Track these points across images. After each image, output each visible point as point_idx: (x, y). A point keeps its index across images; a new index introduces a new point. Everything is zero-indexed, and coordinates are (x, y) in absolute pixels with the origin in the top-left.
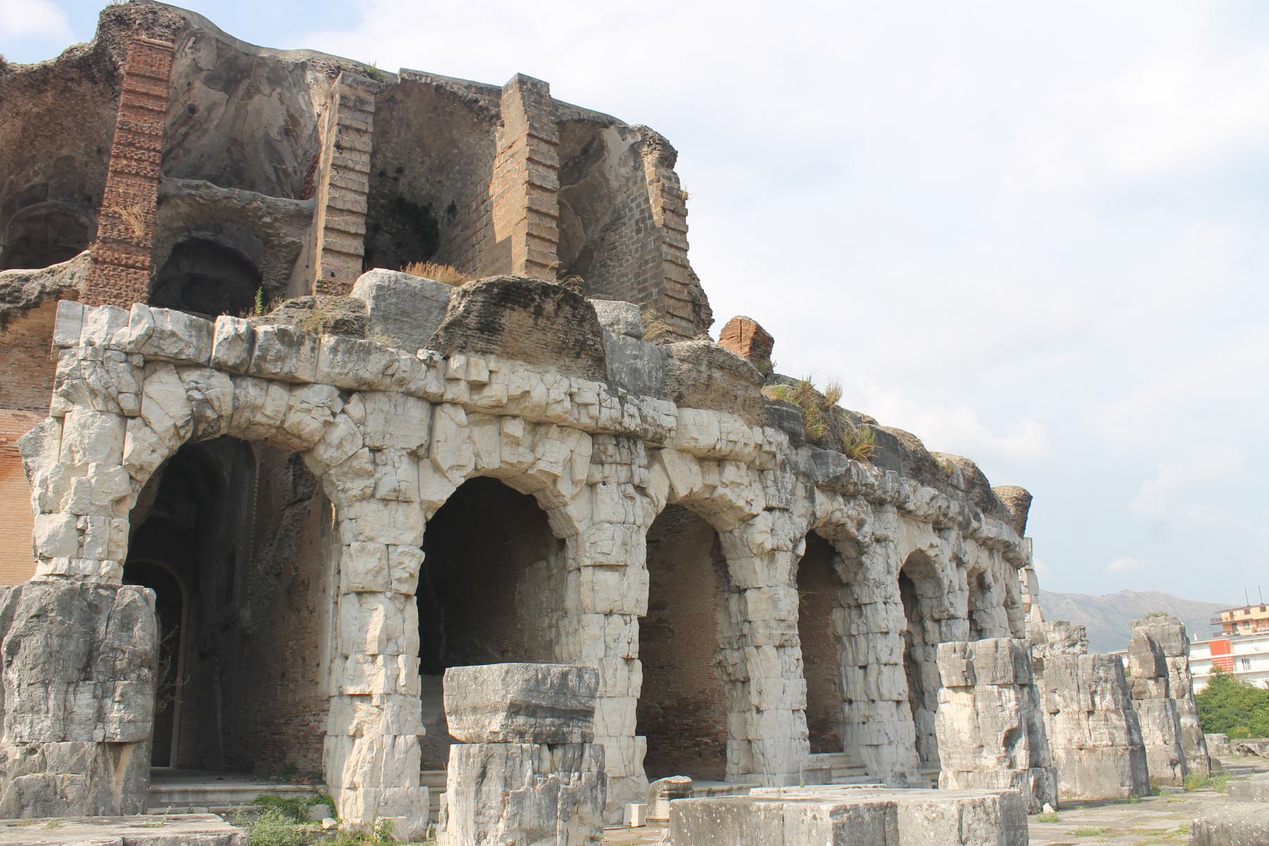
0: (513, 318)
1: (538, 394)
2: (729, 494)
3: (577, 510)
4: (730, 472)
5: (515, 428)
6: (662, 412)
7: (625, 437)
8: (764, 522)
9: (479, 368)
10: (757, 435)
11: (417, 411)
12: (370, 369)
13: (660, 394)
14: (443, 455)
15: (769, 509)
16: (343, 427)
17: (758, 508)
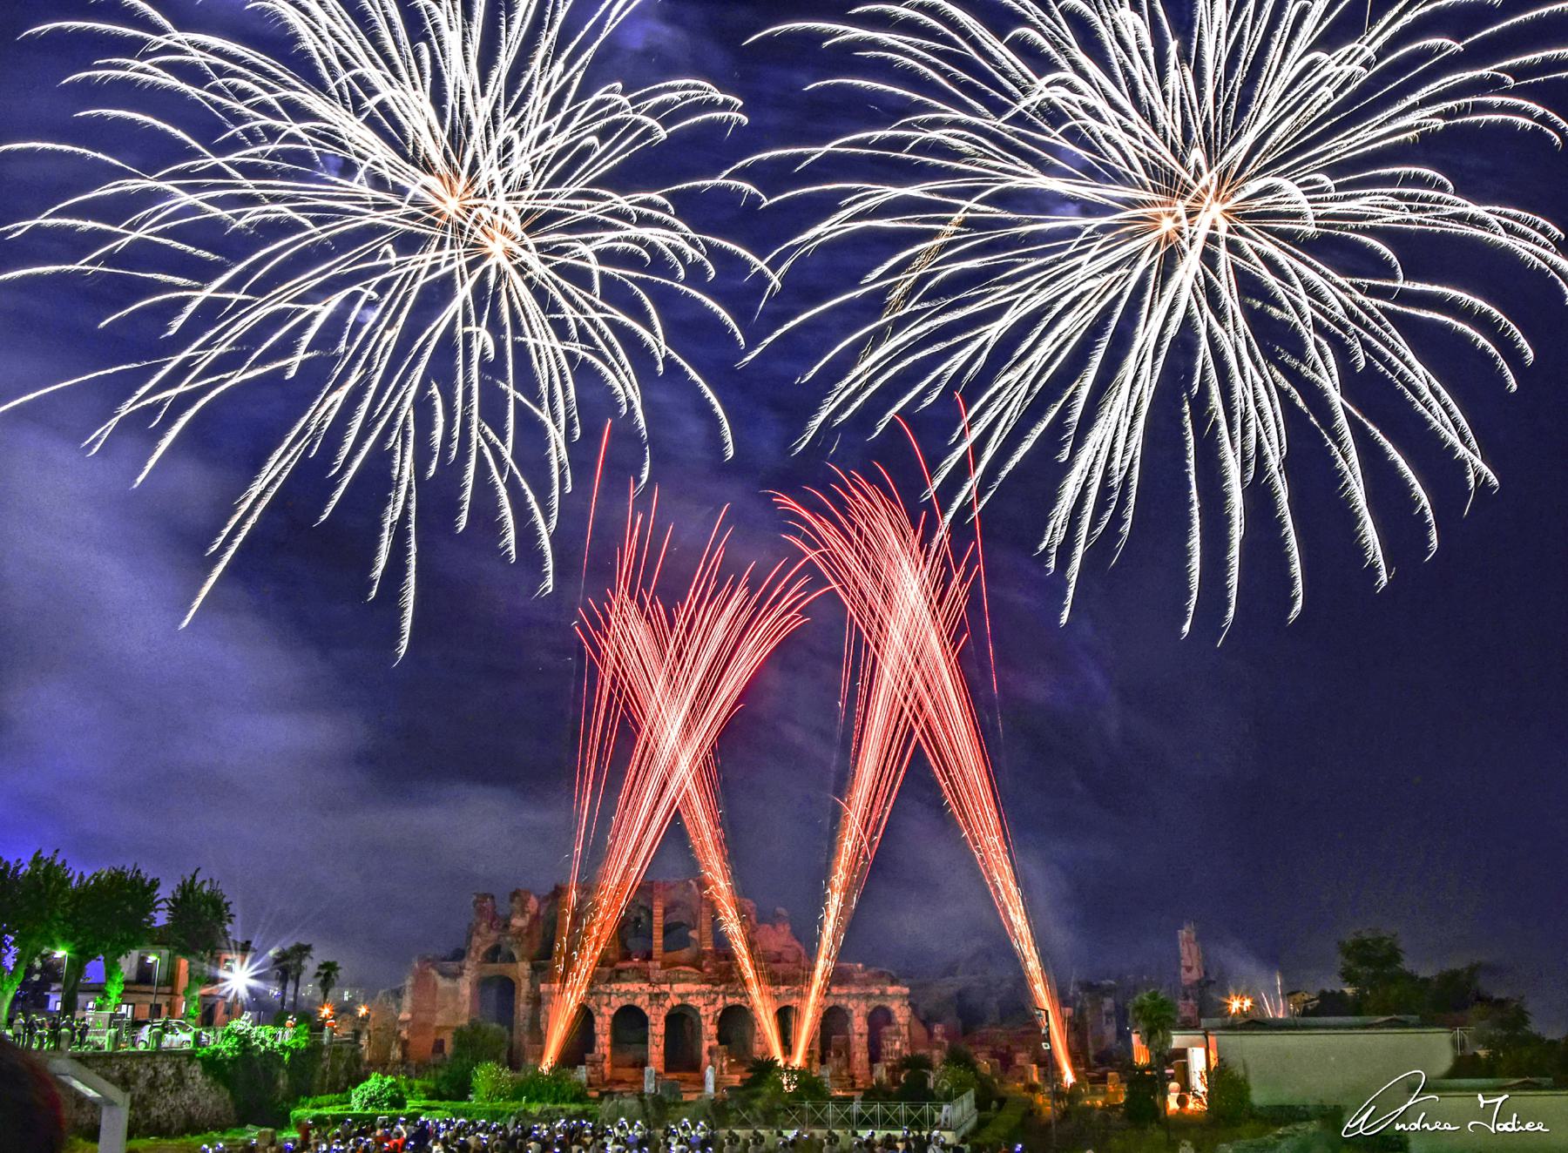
0: (624, 975)
1: (632, 989)
2: (691, 1003)
3: (647, 1012)
4: (690, 998)
5: (628, 996)
6: (665, 987)
7: (657, 995)
8: (703, 1009)
9: (618, 986)
10: (698, 987)
11: (605, 996)
12: (595, 990)
13: (666, 983)
14: (613, 1004)
15: (705, 1005)
16: (591, 1001)
17: (701, 1005)
